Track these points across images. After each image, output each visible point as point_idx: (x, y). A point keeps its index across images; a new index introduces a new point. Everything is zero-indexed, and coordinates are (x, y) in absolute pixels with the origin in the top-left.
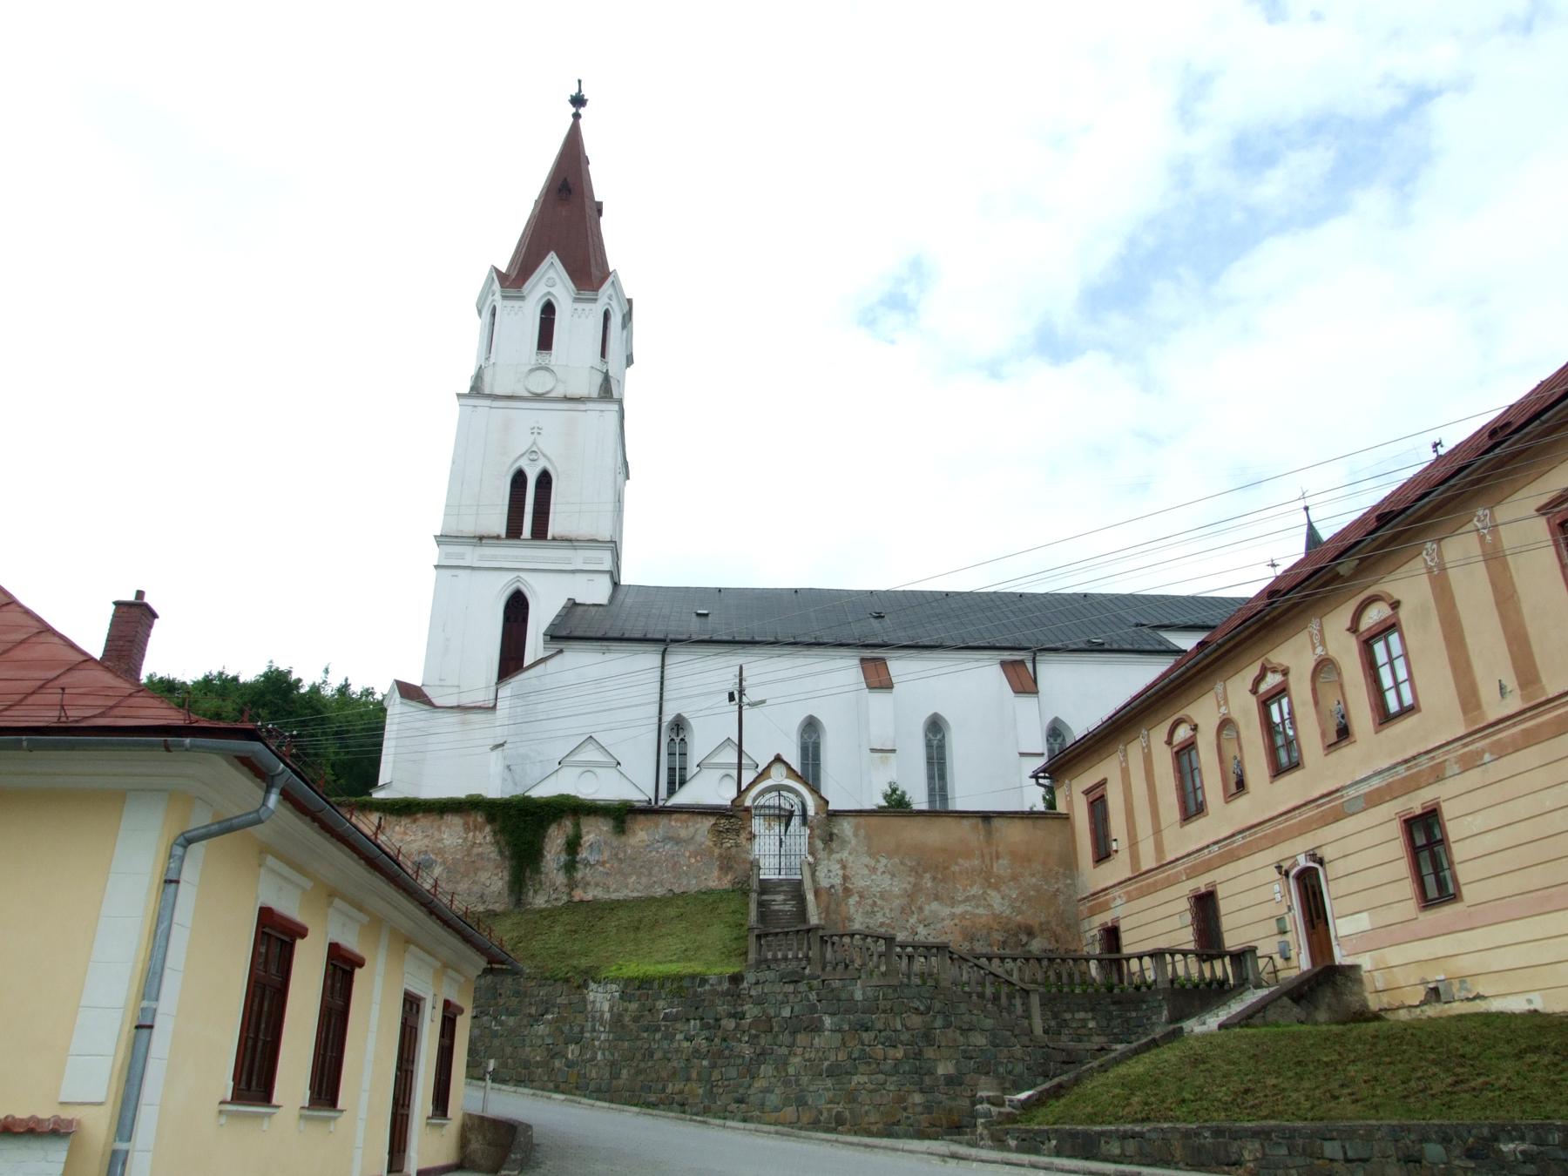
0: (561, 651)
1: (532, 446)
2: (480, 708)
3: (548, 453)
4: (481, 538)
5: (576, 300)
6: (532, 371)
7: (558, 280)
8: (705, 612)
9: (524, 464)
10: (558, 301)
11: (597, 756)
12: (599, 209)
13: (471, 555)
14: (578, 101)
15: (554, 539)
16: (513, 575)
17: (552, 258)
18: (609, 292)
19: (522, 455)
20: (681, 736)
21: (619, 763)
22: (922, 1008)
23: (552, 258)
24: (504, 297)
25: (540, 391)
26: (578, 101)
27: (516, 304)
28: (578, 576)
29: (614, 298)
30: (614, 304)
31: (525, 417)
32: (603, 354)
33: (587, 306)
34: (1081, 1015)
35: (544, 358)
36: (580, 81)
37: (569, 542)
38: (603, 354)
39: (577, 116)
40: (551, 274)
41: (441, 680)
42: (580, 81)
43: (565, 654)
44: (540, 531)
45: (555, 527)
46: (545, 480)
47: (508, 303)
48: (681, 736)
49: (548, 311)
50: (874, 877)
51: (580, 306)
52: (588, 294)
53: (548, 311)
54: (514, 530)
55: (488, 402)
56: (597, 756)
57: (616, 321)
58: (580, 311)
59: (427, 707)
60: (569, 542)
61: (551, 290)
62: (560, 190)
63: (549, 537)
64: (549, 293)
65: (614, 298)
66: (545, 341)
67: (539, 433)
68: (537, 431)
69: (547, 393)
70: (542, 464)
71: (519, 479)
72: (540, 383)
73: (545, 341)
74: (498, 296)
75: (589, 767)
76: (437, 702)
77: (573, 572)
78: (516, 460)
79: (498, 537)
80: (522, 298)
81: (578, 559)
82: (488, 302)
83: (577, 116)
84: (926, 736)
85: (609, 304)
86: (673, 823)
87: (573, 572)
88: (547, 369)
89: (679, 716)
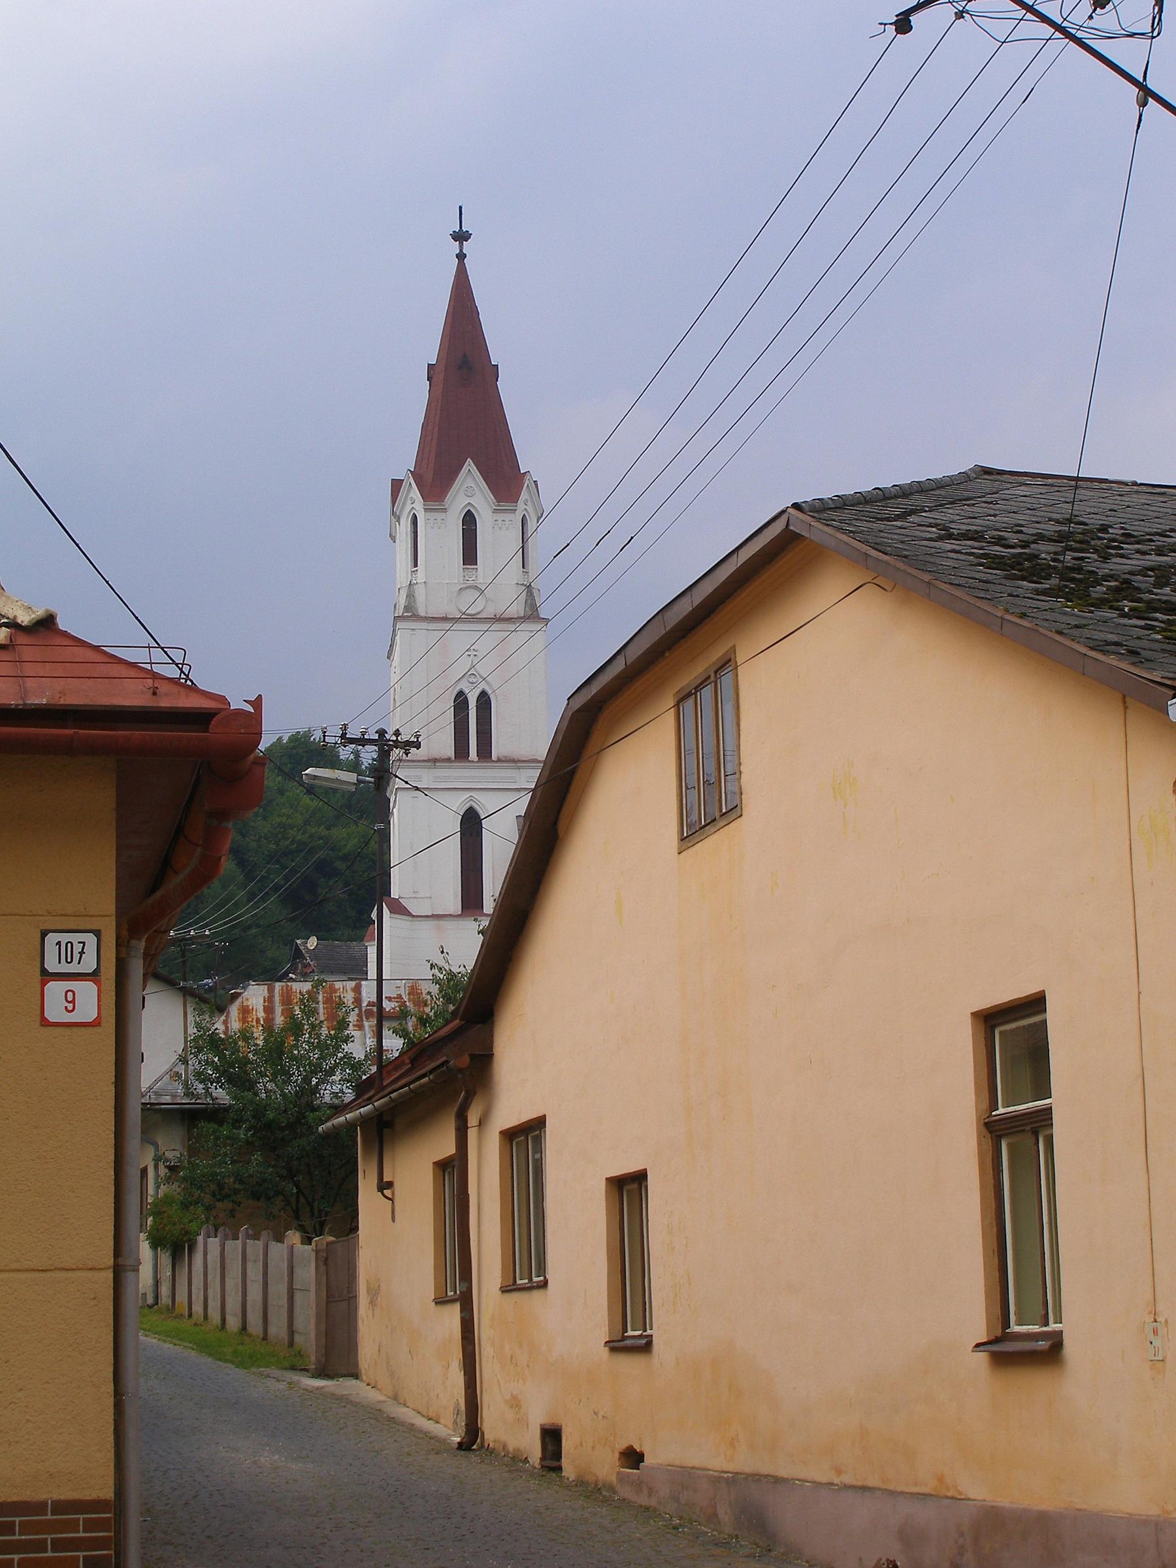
2: (451, 915)
9: (464, 686)
14: (461, 237)
15: (499, 760)
16: (467, 795)
27: (440, 516)
29: (529, 501)
31: (461, 638)
33: (507, 517)
36: (460, 208)
39: (461, 257)
42: (460, 208)
46: (484, 701)
49: (469, 521)
51: (500, 517)
53: (469, 521)
54: (461, 752)
55: (424, 625)
58: (500, 522)
59: (410, 919)
62: (460, 368)
63: (494, 757)
65: (529, 501)
66: (470, 556)
69: (478, 613)
70: (483, 686)
71: (461, 702)
73: (470, 556)
76: (414, 914)
79: (448, 760)
80: (445, 510)
83: (461, 257)
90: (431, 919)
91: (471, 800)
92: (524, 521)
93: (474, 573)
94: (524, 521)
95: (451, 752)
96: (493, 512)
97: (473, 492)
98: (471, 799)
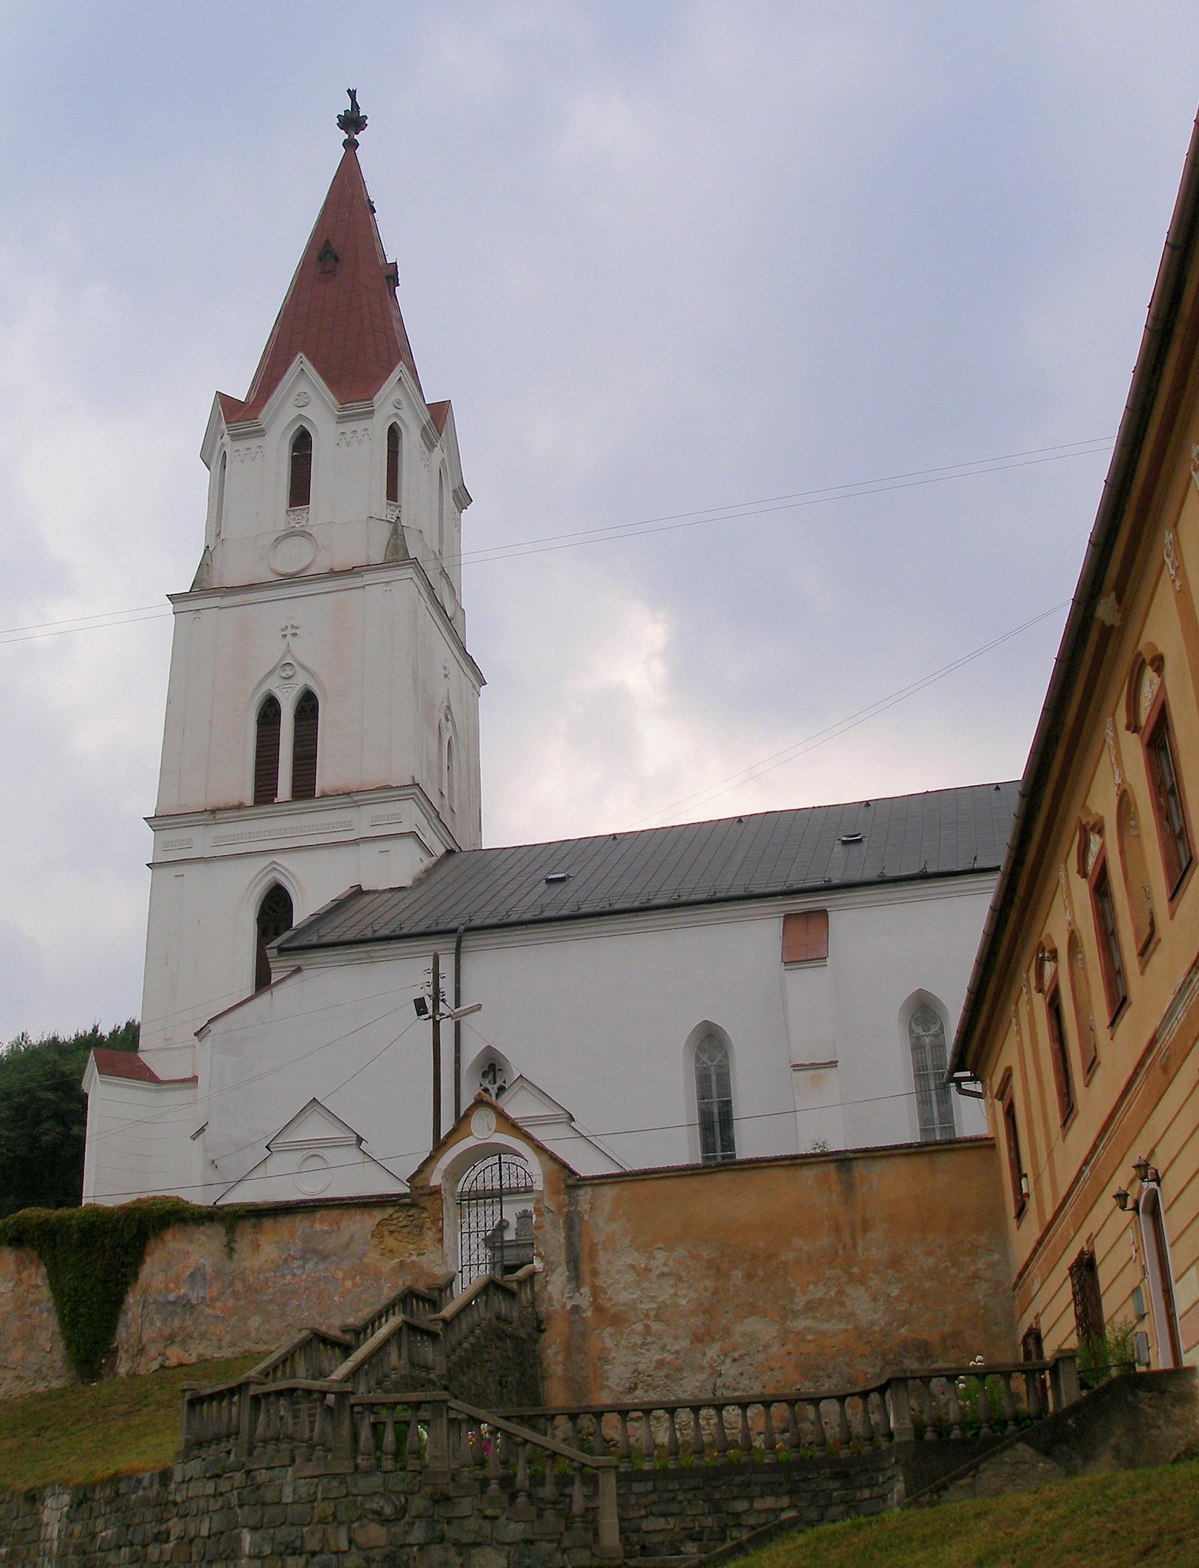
0: (299, 970)
1: (282, 658)
3: (306, 663)
4: (213, 811)
5: (342, 419)
6: (279, 540)
7: (311, 393)
8: (563, 875)
10: (408, 430)
11: (329, 1131)
12: (391, 277)
13: (201, 840)
14: (352, 122)
15: (324, 796)
16: (265, 861)
17: (301, 362)
18: (393, 398)
19: (271, 672)
20: (499, 1083)
21: (360, 1140)
22: (388, 1510)
23: (301, 362)
24: (234, 437)
25: (292, 569)
26: (352, 122)
27: (253, 443)
28: (364, 847)
29: (404, 404)
30: (405, 413)
32: (392, 493)
33: (359, 425)
34: (769, 1502)
35: (299, 520)
37: (349, 796)
38: (392, 493)
39: (351, 145)
40: (303, 387)
41: (166, 1040)
43: (304, 973)
44: (304, 787)
45: (326, 777)
46: (308, 706)
47: (242, 445)
48: (499, 1083)
49: (302, 443)
50: (646, 1284)
51: (348, 427)
52: (358, 407)
53: (302, 443)
54: (265, 791)
56: (329, 1131)
57: (411, 442)
58: (348, 435)
59: (153, 1086)
60: (349, 796)
61: (303, 411)
62: (320, 259)
64: (301, 416)
65: (404, 404)
66: (300, 493)
67: (295, 635)
68: (290, 632)
70: (301, 681)
71: (269, 711)
72: (294, 557)
73: (300, 493)
74: (227, 438)
75: (311, 1149)
77: (356, 842)
78: (261, 683)
79: (240, 807)
80: (261, 433)
81: (363, 820)
82: (218, 448)
83: (351, 145)
84: (911, 1031)
85: (396, 415)
86: (317, 1226)
87: (356, 842)
88: (303, 534)
89: (489, 1051)
90: (188, 1085)
91: (274, 868)
92: (394, 434)
93: (305, 515)
94: (394, 434)
95: (248, 795)
96: (337, 423)
97: (307, 400)
98: (274, 867)
